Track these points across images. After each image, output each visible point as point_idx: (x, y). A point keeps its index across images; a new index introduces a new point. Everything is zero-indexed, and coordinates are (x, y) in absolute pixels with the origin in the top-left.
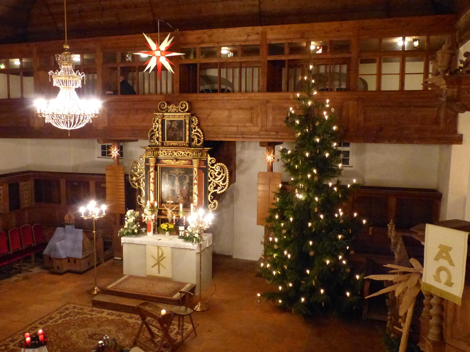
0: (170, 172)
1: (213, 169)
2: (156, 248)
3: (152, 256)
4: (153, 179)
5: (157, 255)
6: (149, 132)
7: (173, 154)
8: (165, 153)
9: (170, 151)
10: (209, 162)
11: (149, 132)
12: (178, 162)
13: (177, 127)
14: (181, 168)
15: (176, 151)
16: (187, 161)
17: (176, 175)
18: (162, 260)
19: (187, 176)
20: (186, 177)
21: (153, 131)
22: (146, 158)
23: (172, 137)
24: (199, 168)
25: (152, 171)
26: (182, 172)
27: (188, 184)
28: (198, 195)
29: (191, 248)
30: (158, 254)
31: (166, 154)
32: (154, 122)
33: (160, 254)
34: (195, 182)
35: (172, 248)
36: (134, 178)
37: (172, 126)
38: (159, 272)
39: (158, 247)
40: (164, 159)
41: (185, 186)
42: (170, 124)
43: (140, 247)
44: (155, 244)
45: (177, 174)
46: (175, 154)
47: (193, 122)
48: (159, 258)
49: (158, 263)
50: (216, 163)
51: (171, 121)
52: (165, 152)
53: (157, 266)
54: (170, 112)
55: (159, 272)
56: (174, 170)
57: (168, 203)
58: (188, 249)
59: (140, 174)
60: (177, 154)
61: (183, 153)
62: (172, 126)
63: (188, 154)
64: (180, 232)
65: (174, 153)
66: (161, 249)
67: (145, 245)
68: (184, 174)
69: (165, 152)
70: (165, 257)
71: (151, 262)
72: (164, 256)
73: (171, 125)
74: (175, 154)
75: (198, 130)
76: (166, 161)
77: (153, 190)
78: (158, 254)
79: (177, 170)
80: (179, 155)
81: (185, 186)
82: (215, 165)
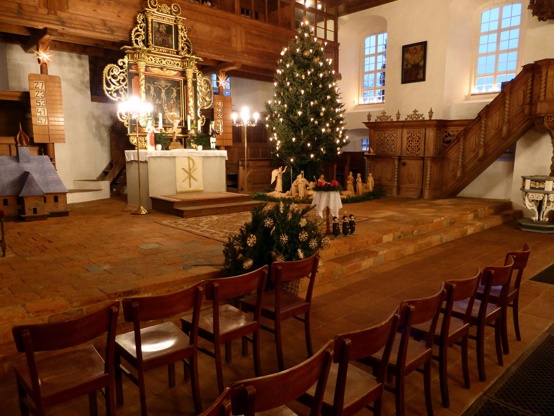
2: (187, 159)
3: (183, 169)
5: (188, 168)
7: (161, 62)
9: (158, 59)
11: (133, 32)
13: (166, 32)
15: (164, 59)
17: (163, 88)
18: (193, 171)
21: (137, 31)
22: (128, 64)
23: (160, 41)
26: (169, 84)
27: (176, 98)
30: (189, 165)
31: (153, 61)
33: (191, 165)
37: (160, 29)
38: (190, 186)
39: (189, 157)
40: (151, 67)
42: (157, 26)
45: (163, 86)
46: (164, 62)
48: (190, 170)
49: (190, 176)
51: (159, 24)
52: (153, 59)
53: (188, 179)
54: (162, 12)
55: (190, 186)
56: (160, 82)
61: (172, 62)
62: (160, 29)
63: (178, 65)
65: (163, 60)
66: (192, 160)
67: (175, 157)
68: (170, 86)
69: (153, 59)
71: (181, 175)
73: (159, 28)
74: (164, 62)
76: (155, 69)
78: (189, 165)
79: (163, 82)
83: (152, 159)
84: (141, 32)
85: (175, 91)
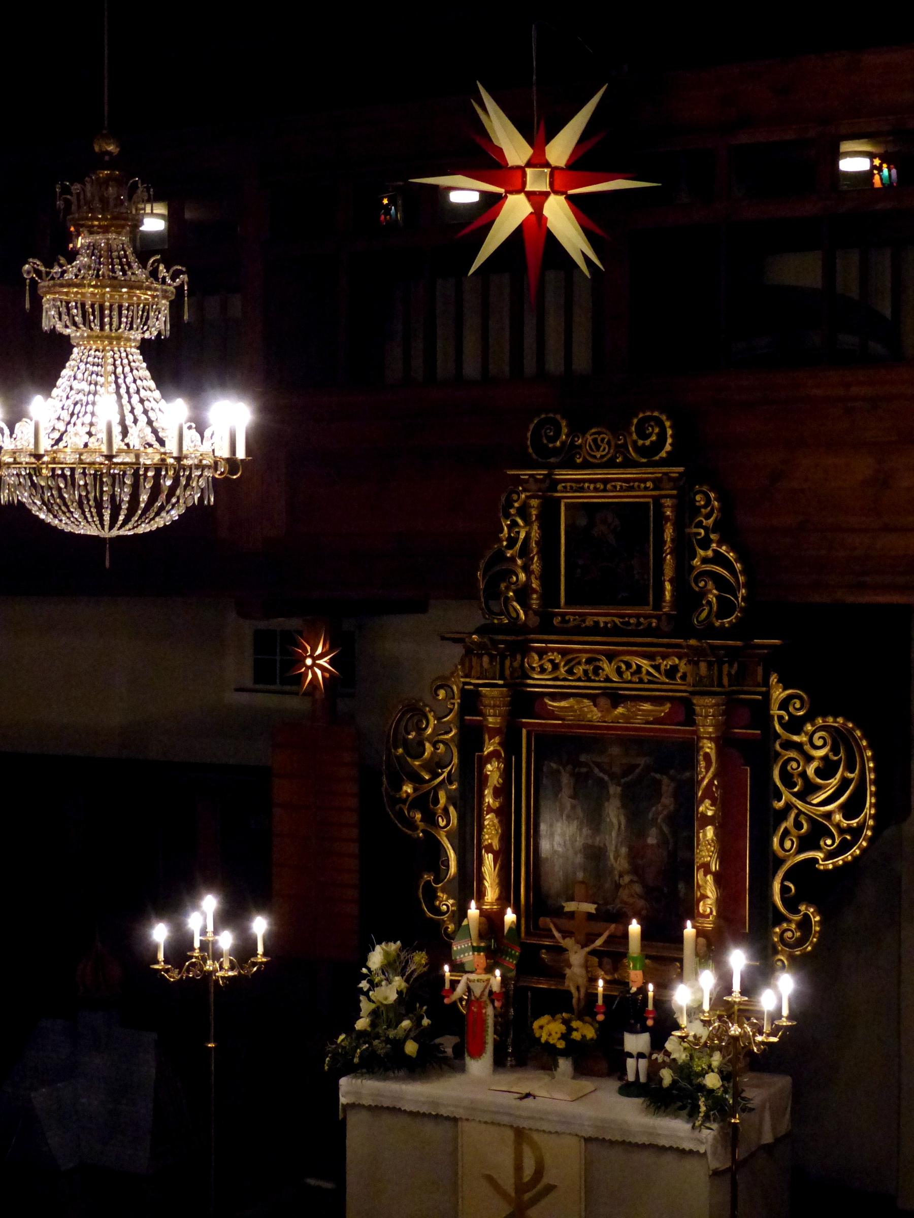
0: (583, 758)
1: (798, 747)
3: (490, 1179)
4: (497, 793)
6: (482, 564)
8: (556, 667)
9: (584, 657)
10: (775, 712)
11: (482, 564)
12: (620, 710)
14: (634, 742)
15: (610, 657)
16: (667, 707)
17: (612, 776)
18: (535, 1201)
19: (665, 780)
20: (659, 782)
21: (500, 556)
22: (463, 691)
24: (724, 742)
25: (495, 754)
26: (642, 761)
27: (671, 819)
28: (719, 879)
29: (687, 1145)
30: (519, 1168)
32: (507, 516)
33: (528, 1171)
34: (707, 809)
35: (588, 1140)
36: (408, 789)
39: (520, 1134)
40: (554, 697)
41: (654, 831)
42: (582, 522)
43: (429, 1128)
44: (505, 1120)
45: (616, 769)
46: (608, 668)
47: (697, 511)
48: (521, 1188)
50: (810, 717)
54: (586, 465)
57: (572, 915)
58: (671, 1148)
59: (434, 766)
60: (619, 672)
61: (645, 663)
63: (672, 672)
64: (630, 1063)
66: (534, 1147)
67: (455, 1120)
69: (558, 658)
70: (550, 1188)
72: (545, 1181)
74: (608, 668)
75: (723, 549)
76: (563, 704)
77: (496, 845)
78: (519, 1168)
79: (615, 750)
80: (627, 675)
81: (654, 831)
82: (809, 727)
83: (364, 1115)
84: (513, 559)
85: (667, 787)
